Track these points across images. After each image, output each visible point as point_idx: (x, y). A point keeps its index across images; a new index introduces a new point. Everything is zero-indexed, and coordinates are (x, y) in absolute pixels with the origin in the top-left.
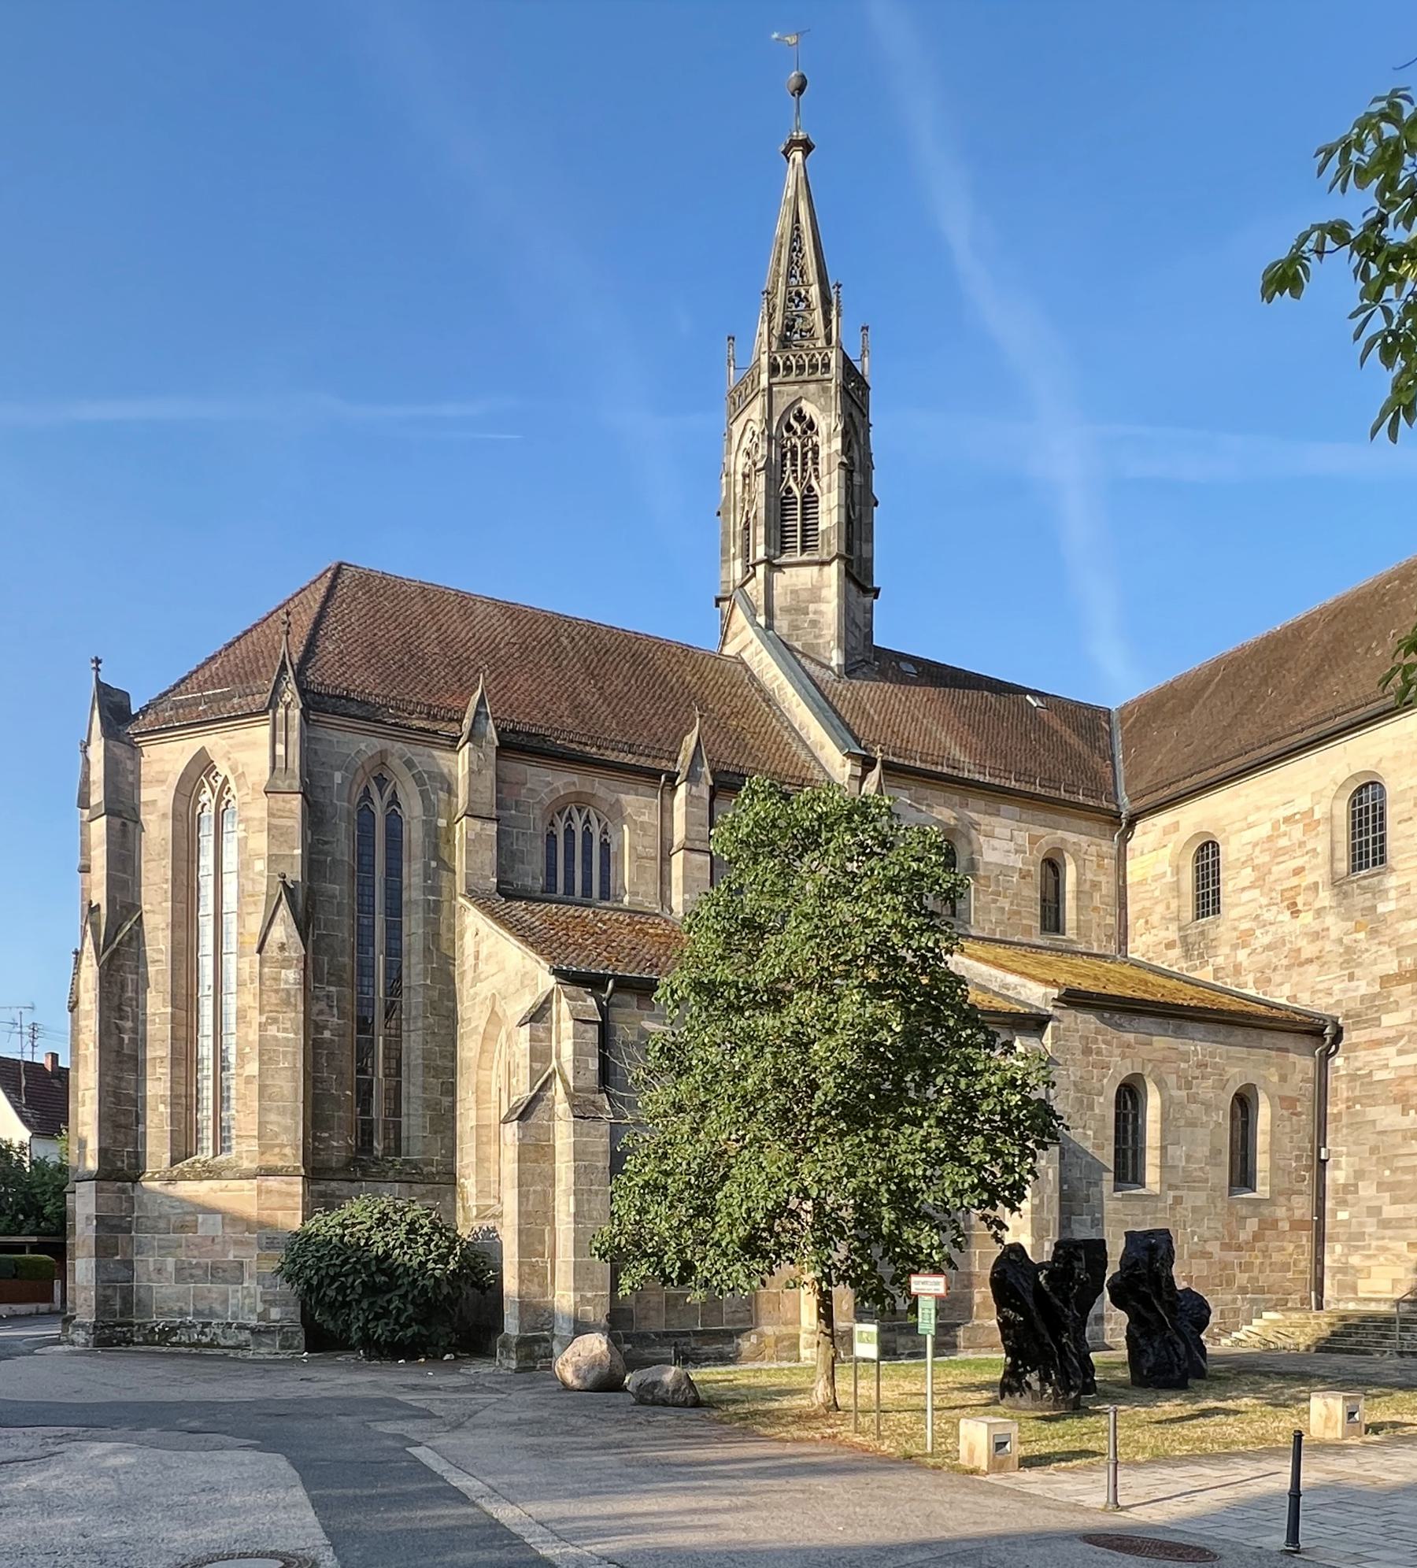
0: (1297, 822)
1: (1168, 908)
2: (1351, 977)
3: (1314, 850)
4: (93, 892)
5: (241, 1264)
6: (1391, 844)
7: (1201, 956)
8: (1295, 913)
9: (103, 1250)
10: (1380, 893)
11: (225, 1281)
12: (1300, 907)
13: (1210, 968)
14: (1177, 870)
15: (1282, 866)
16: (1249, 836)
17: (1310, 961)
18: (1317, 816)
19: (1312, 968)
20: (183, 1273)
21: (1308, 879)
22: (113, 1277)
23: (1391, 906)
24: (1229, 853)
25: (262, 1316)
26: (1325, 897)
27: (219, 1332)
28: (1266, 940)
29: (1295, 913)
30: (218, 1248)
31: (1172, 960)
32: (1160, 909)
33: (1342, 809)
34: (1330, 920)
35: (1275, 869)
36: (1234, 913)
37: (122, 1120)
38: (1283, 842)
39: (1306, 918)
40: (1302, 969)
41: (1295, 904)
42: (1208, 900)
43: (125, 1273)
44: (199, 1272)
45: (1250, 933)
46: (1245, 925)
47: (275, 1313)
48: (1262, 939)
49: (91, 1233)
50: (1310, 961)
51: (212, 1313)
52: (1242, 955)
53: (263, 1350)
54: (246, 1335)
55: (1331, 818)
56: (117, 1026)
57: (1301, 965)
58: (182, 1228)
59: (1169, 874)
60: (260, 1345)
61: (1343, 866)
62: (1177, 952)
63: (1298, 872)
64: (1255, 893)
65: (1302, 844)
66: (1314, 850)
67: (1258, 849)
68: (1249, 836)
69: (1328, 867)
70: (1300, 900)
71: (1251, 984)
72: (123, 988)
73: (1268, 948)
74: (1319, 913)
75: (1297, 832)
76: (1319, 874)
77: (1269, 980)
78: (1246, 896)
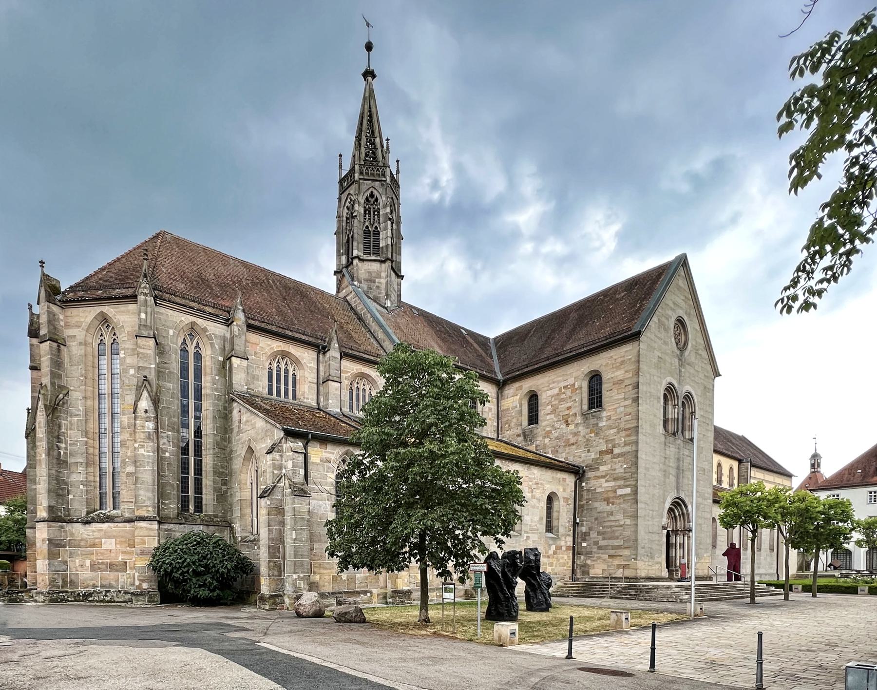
4: (43, 379)
5: (126, 563)
6: (604, 399)
7: (531, 440)
8: (568, 425)
9: (52, 555)
10: (599, 418)
11: (117, 571)
14: (521, 405)
16: (550, 393)
17: (573, 444)
20: (94, 567)
22: (58, 569)
23: (604, 424)
24: (543, 398)
25: (139, 587)
26: (579, 419)
27: (115, 595)
28: (556, 435)
29: (568, 425)
30: (113, 555)
31: (519, 442)
32: (514, 420)
33: (585, 385)
34: (581, 428)
36: (544, 424)
37: (61, 492)
38: (563, 396)
39: (572, 427)
42: (533, 418)
43: (64, 567)
44: (104, 567)
46: (548, 429)
47: (145, 586)
48: (555, 434)
49: (45, 547)
50: (573, 444)
51: (111, 586)
52: (547, 440)
53: (139, 603)
54: (128, 596)
55: (581, 388)
56: (57, 446)
58: (94, 545)
60: (138, 601)
61: (585, 407)
62: (521, 439)
63: (569, 408)
65: (570, 397)
68: (550, 393)
70: (569, 420)
72: (60, 427)
74: (577, 425)
75: (569, 392)
76: (576, 410)
78: (548, 417)
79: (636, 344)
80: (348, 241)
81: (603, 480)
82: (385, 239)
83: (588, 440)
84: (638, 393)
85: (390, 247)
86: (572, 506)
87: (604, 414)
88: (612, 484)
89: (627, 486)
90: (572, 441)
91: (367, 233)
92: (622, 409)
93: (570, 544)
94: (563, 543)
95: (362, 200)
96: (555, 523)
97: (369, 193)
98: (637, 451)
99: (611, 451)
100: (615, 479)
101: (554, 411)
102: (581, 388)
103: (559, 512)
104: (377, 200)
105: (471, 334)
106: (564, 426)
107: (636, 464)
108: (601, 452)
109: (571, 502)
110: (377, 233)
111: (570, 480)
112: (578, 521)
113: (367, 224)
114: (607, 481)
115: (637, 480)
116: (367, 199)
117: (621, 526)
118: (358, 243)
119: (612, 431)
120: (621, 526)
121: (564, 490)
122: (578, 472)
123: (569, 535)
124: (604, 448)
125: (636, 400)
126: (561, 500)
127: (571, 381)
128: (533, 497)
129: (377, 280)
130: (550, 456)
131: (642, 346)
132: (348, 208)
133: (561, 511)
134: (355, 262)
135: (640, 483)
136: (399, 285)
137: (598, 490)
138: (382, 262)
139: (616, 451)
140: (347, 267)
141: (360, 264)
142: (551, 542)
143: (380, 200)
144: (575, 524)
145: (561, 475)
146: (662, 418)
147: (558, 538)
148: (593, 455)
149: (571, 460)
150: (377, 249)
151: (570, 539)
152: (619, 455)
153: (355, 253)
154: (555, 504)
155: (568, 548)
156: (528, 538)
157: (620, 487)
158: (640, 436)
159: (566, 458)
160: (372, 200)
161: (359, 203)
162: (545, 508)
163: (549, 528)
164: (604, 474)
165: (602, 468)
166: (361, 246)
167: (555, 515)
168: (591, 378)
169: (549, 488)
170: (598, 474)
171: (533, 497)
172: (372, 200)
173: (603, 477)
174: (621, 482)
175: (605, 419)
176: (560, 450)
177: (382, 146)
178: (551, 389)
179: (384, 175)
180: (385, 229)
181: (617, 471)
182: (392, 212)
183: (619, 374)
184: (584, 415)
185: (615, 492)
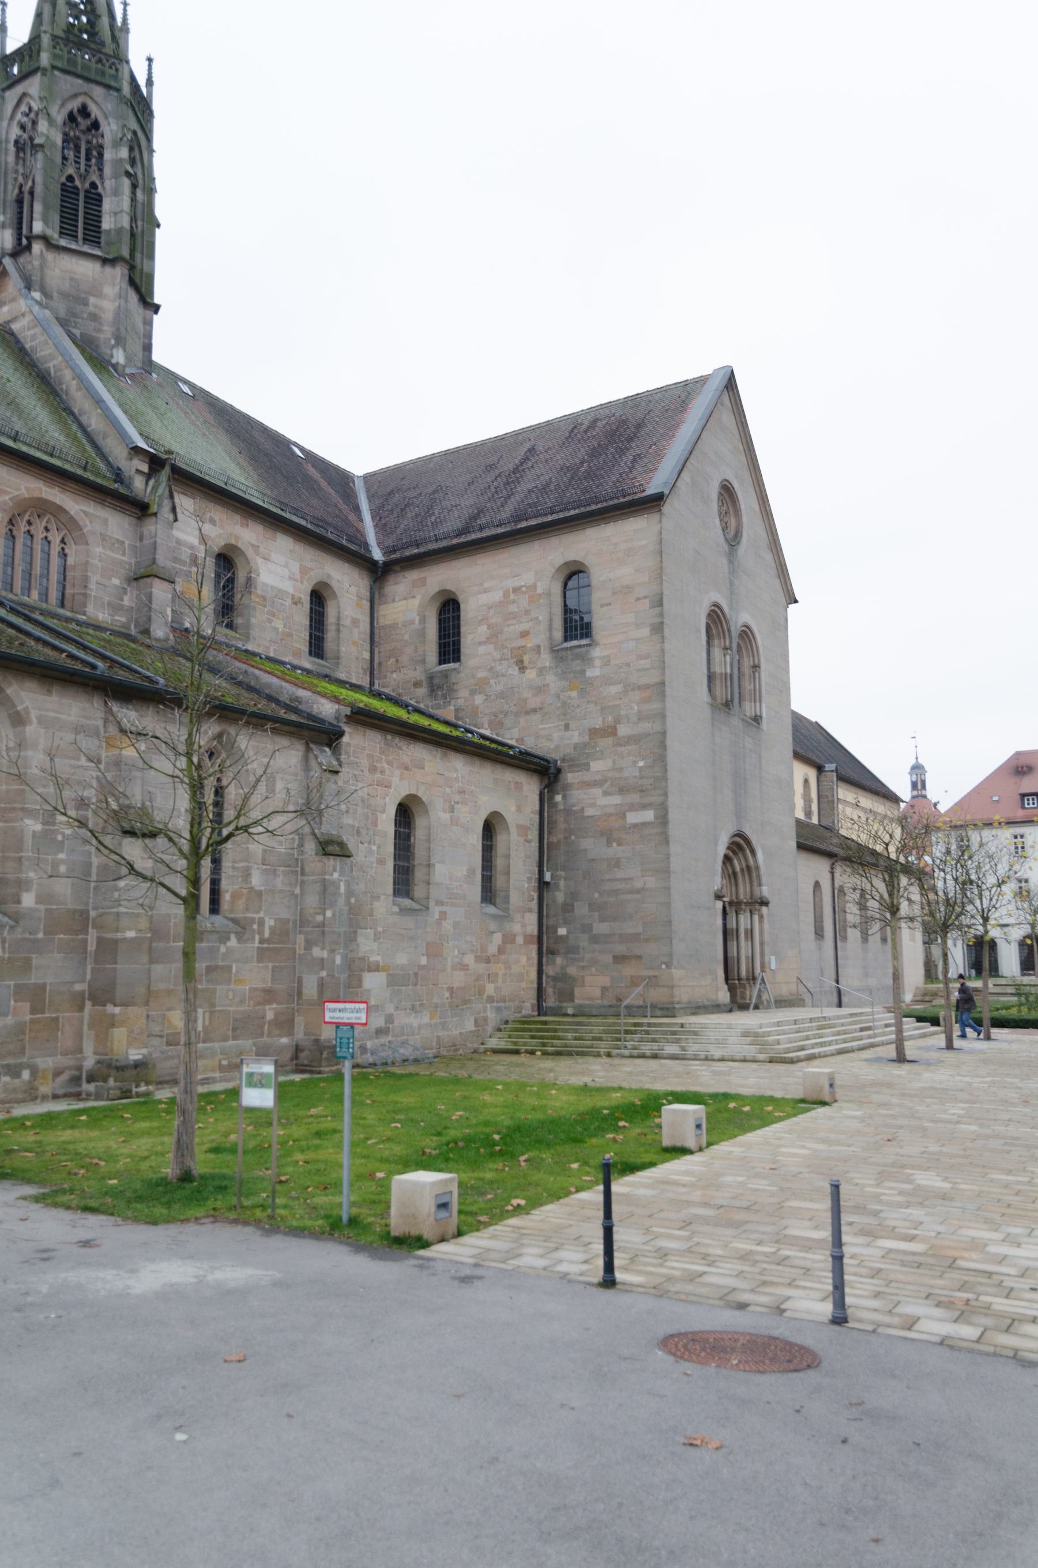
0: (524, 593)
1: (416, 651)
2: (567, 727)
3: (537, 618)
7: (444, 697)
8: (522, 669)
12: (526, 664)
13: (452, 708)
14: (423, 620)
15: (512, 628)
16: (484, 599)
17: (534, 711)
18: (539, 591)
19: (536, 717)
21: (530, 643)
26: (546, 659)
28: (500, 688)
29: (522, 669)
31: (419, 696)
32: (409, 650)
34: (550, 678)
35: (506, 629)
38: (513, 608)
39: (531, 674)
40: (528, 717)
41: (522, 661)
42: (450, 648)
45: (485, 681)
46: (481, 674)
48: (496, 686)
50: (534, 711)
52: (479, 699)
57: (528, 713)
59: (417, 621)
61: (558, 634)
62: (422, 691)
63: (524, 634)
64: (490, 648)
65: (527, 612)
66: (537, 618)
67: (492, 611)
68: (484, 599)
69: (548, 634)
70: (526, 658)
71: (486, 726)
73: (502, 695)
74: (541, 671)
76: (539, 638)
77: (502, 724)
78: (482, 649)
79: (654, 517)
80: (20, 201)
81: (597, 792)
82: (114, 215)
83: (564, 704)
84: (661, 615)
85: (126, 238)
86: (535, 844)
87: (596, 652)
88: (616, 800)
89: (644, 807)
90: (533, 702)
91: (68, 190)
92: (631, 645)
93: (533, 929)
94: (517, 928)
95: (60, 117)
96: (499, 881)
97: (75, 105)
98: (664, 733)
99: (610, 731)
100: (622, 790)
101: (494, 637)
102: (548, 594)
103: (508, 856)
104: (96, 125)
105: (312, 458)
106: (514, 671)
107: (661, 759)
108: (593, 732)
109: (534, 835)
110: (94, 199)
111: (530, 787)
112: (548, 877)
113: (71, 171)
114: (606, 794)
115: (666, 795)
116: (71, 118)
117: (638, 892)
118: (46, 207)
119: (614, 689)
120: (638, 892)
121: (519, 809)
122: (546, 772)
123: (530, 911)
124: (598, 723)
125: (658, 628)
126: (513, 829)
127: (527, 578)
128: (454, 821)
129: (92, 300)
130: (487, 733)
131: (668, 523)
132: (23, 127)
133: (513, 853)
134: (37, 247)
135: (672, 800)
136: (149, 323)
137: (589, 812)
138: (105, 261)
139: (623, 730)
140: (15, 255)
141: (50, 256)
142: (493, 926)
143: (104, 128)
144: (543, 886)
145: (511, 776)
146: (705, 671)
147: (505, 917)
148: (575, 737)
149: (529, 744)
150: (93, 233)
151: (532, 919)
152: (630, 740)
153: (38, 227)
154: (501, 840)
155: (527, 939)
156: (443, 915)
157: (632, 807)
158: (669, 704)
159: (520, 740)
160: (84, 123)
161: (51, 121)
162: (480, 848)
163: (489, 893)
164: (598, 777)
165: (596, 766)
166: (56, 218)
167: (499, 863)
168: (569, 577)
169: (488, 803)
170: (587, 777)
171: (454, 821)
172: (84, 123)
173: (595, 784)
174: (634, 798)
175: (597, 663)
176: (508, 722)
177: (112, 16)
178: (486, 591)
179: (116, 78)
180: (116, 192)
181: (626, 774)
182: (133, 162)
183: (625, 573)
184: (554, 650)
185: (624, 817)
